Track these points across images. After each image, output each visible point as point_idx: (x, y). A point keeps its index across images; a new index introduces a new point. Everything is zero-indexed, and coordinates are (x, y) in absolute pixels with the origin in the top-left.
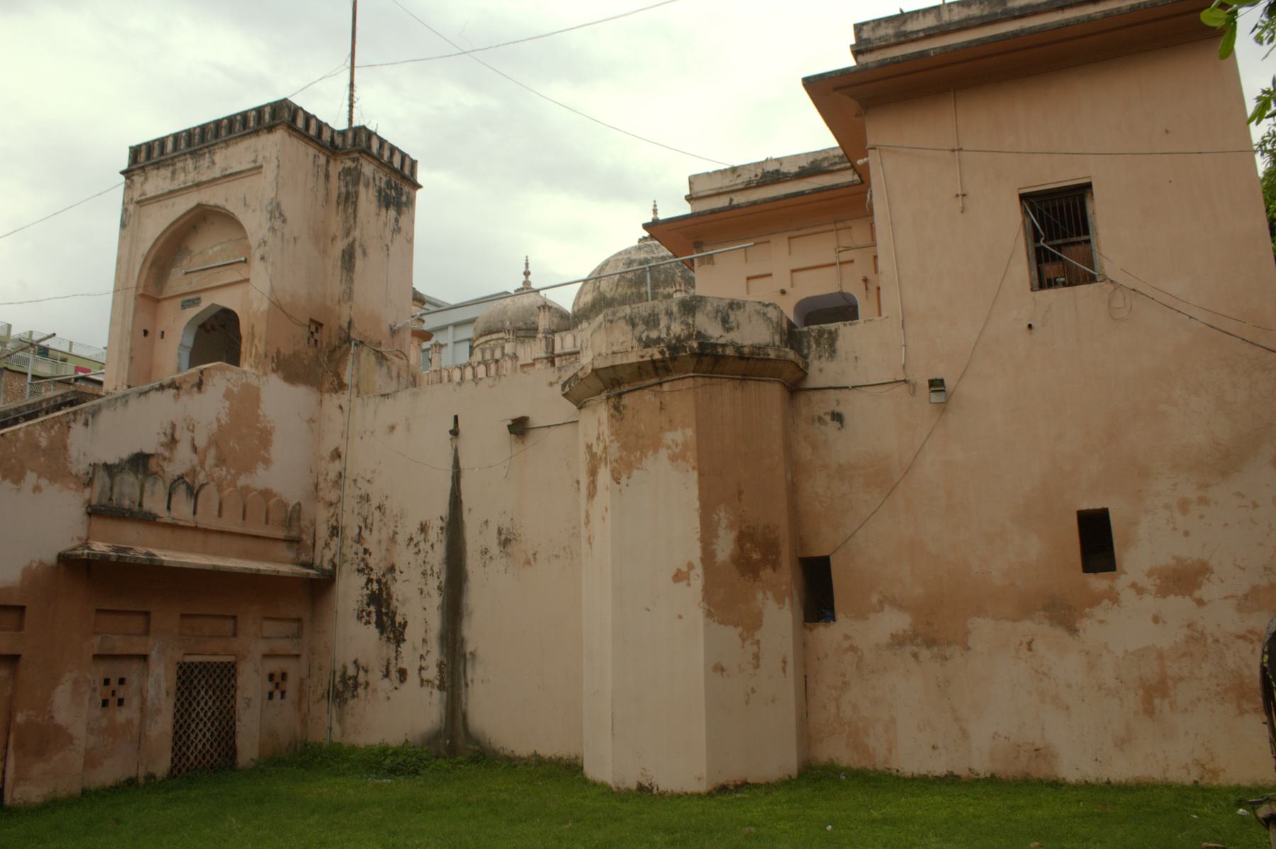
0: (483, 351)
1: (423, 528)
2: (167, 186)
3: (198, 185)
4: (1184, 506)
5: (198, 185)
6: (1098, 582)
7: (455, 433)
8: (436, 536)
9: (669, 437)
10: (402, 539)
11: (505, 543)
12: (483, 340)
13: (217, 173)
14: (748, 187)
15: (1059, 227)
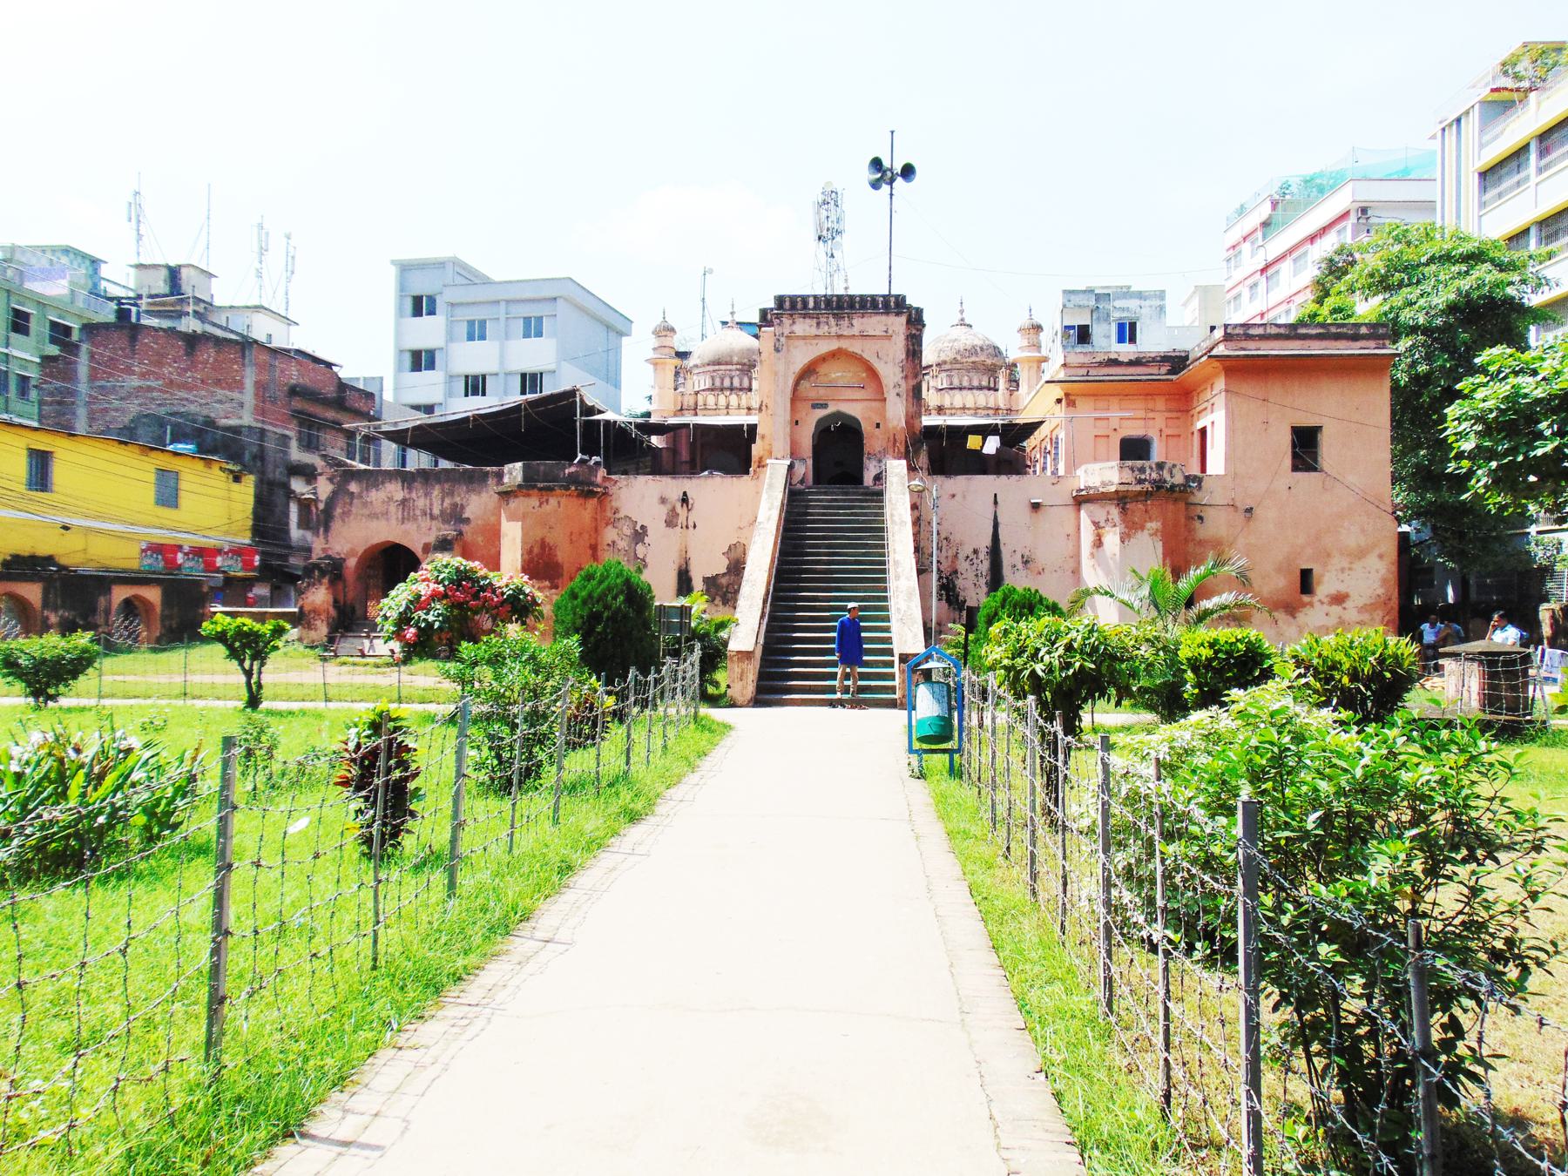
0: (713, 379)
1: (976, 552)
2: (814, 331)
3: (839, 336)
4: (1343, 570)
5: (839, 336)
6: (1306, 598)
7: (996, 503)
8: (982, 556)
9: (1149, 525)
10: (961, 556)
11: (1026, 563)
12: (711, 368)
13: (855, 331)
14: (1100, 364)
15: (1305, 446)
